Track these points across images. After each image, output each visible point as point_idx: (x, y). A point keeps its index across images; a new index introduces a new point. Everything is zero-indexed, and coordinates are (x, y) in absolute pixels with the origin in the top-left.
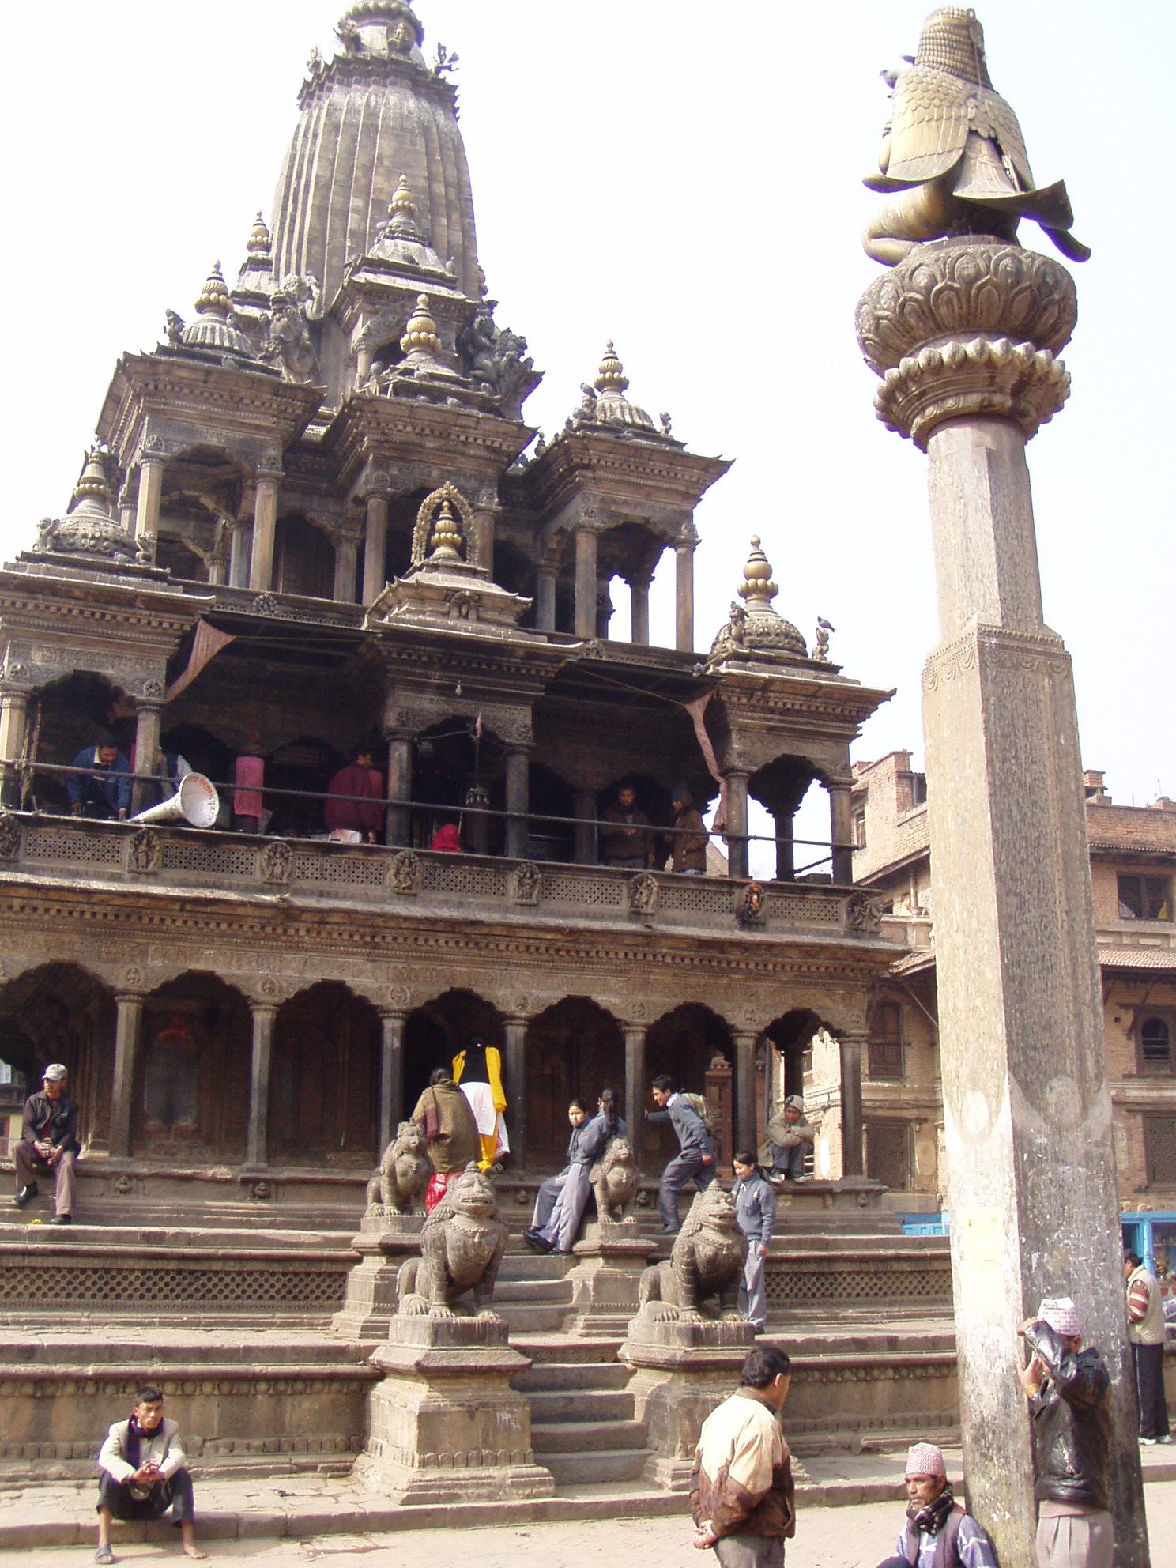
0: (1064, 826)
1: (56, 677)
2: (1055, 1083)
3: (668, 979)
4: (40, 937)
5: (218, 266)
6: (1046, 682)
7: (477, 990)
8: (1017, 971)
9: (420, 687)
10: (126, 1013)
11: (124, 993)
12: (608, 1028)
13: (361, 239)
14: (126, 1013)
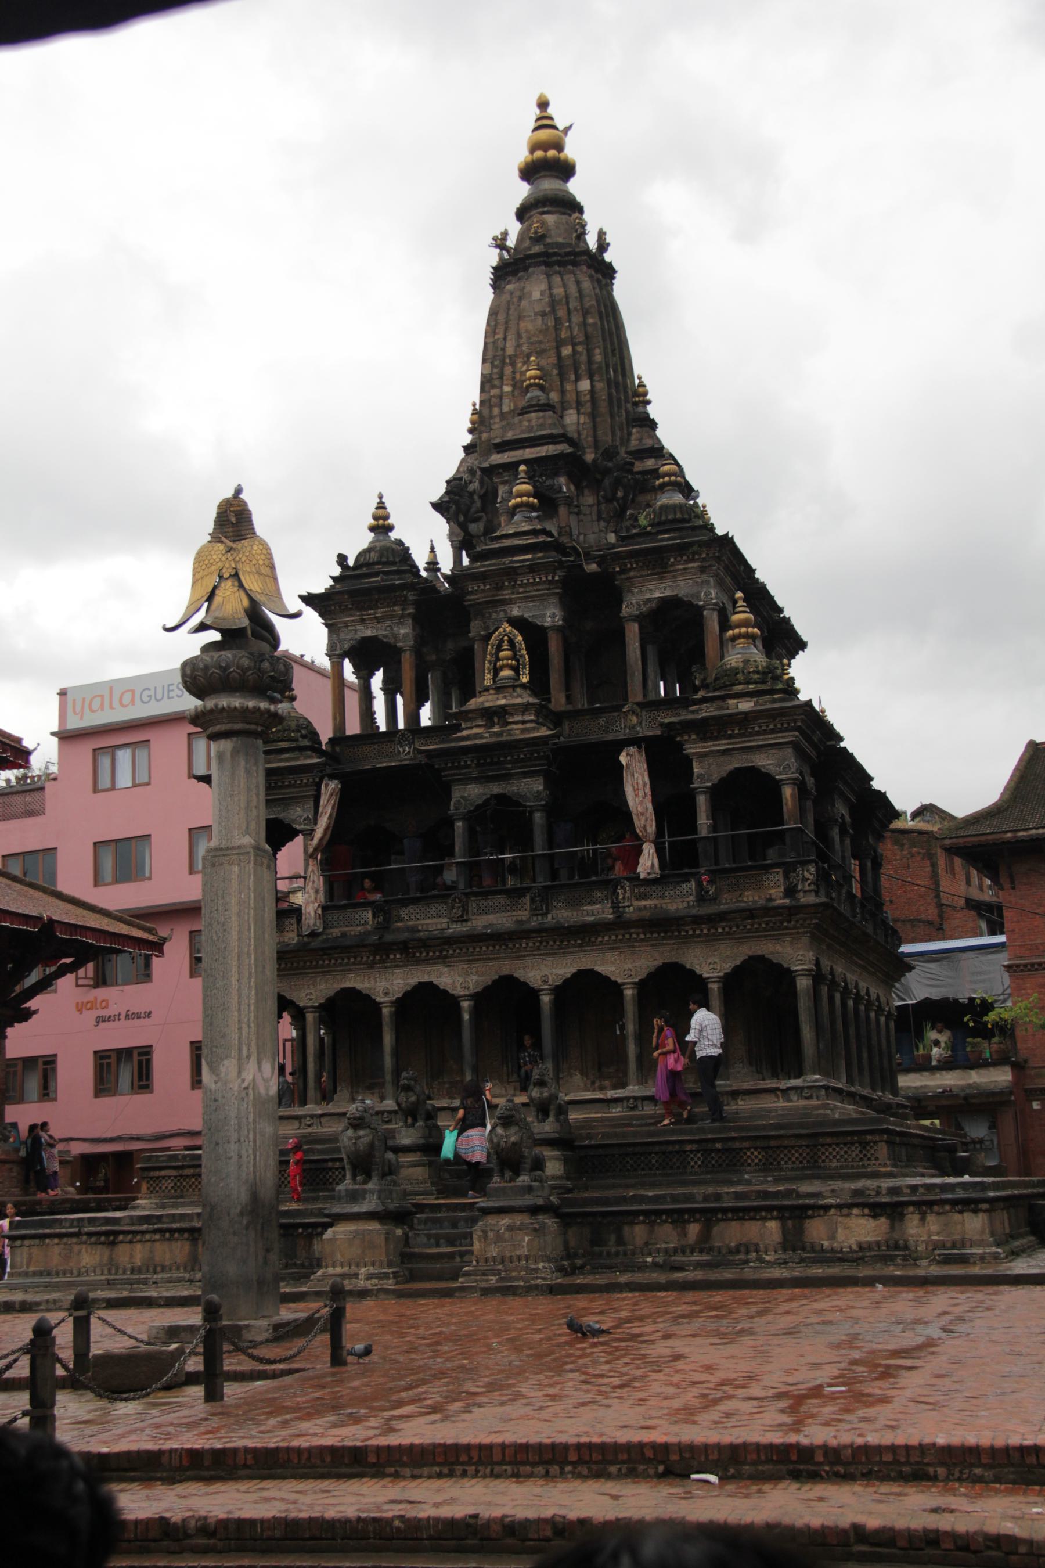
0: (239, 939)
2: (226, 1062)
5: (381, 497)
6: (236, 869)
7: (516, 975)
8: (210, 1012)
9: (466, 780)
11: (308, 1007)
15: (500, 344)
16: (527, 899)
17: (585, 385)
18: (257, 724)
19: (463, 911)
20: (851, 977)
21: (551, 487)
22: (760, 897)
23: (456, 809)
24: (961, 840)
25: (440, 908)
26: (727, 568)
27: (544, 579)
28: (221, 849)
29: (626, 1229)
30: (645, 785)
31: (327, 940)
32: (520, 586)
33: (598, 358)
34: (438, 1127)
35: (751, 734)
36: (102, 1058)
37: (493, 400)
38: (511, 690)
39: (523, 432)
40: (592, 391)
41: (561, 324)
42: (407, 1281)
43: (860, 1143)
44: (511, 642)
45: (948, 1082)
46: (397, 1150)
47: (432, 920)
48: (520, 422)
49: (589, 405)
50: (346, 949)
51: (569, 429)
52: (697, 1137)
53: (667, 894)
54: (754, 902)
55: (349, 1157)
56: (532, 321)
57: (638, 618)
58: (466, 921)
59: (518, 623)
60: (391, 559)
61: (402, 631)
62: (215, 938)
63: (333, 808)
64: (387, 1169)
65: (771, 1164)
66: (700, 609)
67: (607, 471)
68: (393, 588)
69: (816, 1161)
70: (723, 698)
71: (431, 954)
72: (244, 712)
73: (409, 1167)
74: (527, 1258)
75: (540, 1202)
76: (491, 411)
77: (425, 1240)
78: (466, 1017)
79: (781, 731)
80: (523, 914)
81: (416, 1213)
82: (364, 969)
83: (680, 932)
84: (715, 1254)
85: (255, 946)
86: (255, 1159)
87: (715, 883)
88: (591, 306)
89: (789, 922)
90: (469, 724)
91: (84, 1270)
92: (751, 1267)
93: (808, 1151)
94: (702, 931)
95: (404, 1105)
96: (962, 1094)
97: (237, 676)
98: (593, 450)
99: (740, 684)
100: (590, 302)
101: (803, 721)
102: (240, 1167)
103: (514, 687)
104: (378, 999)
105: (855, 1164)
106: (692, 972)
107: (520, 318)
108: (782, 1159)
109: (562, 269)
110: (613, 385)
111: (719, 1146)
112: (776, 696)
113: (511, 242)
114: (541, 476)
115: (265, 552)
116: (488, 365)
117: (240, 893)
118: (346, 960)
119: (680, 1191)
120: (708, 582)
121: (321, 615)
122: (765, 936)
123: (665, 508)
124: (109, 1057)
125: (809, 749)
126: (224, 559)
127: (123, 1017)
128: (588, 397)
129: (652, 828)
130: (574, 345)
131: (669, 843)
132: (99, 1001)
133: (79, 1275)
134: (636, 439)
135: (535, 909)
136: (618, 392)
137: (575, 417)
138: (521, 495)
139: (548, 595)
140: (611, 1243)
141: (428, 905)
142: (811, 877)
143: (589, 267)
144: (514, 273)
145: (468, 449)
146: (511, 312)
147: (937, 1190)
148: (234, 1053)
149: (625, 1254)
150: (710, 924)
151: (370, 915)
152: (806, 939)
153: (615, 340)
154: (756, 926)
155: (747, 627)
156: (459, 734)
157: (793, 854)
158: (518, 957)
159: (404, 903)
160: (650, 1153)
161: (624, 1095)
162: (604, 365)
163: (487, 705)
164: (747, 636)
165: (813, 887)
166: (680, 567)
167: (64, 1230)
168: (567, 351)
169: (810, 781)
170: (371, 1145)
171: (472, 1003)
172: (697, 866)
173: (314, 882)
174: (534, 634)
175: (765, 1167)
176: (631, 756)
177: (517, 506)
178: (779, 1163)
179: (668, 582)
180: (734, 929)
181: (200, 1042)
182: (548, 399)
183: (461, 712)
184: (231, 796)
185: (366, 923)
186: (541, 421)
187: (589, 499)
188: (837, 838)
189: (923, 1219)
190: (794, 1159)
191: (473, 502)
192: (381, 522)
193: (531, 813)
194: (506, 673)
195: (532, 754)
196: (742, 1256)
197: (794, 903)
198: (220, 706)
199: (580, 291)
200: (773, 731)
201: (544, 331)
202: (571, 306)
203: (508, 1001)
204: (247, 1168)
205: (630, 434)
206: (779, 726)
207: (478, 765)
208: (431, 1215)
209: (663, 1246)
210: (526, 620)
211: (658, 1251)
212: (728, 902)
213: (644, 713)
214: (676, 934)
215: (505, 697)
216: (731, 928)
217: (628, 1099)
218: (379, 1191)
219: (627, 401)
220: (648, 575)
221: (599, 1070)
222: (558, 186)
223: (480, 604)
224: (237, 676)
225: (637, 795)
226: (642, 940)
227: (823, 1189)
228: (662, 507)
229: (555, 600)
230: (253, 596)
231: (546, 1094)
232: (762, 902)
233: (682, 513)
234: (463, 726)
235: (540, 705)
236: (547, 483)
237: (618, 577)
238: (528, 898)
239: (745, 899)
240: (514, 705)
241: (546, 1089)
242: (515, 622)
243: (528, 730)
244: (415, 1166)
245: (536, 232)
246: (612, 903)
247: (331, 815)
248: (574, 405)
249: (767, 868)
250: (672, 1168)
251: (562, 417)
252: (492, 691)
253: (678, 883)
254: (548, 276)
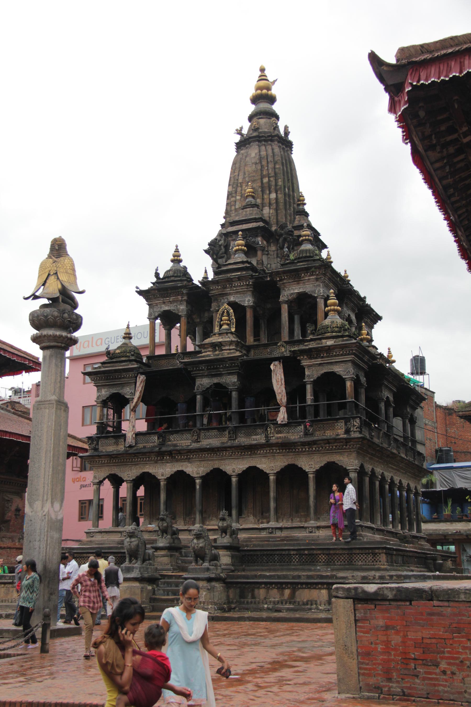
0: (47, 444)
1: (108, 396)
2: (37, 502)
4: (107, 468)
5: (177, 247)
6: (47, 411)
7: (221, 468)
9: (203, 376)
12: (264, 476)
15: (236, 177)
16: (227, 433)
17: (273, 196)
18: (62, 343)
19: (198, 437)
20: (388, 475)
21: (254, 242)
22: (333, 434)
23: (198, 389)
24: (467, 413)
25: (188, 436)
26: (329, 279)
27: (245, 284)
28: (42, 402)
29: (256, 591)
30: (281, 380)
31: (137, 449)
32: (234, 287)
33: (280, 183)
34: (179, 539)
35: (332, 356)
36: (82, 503)
37: (232, 203)
38: (225, 334)
39: (243, 217)
40: (277, 199)
41: (264, 168)
42: (151, 612)
43: (373, 554)
44: (228, 312)
45: (459, 528)
46: (157, 549)
47: (183, 441)
48: (242, 212)
49: (275, 204)
50: (144, 454)
51: (265, 216)
52: (296, 548)
53: (290, 431)
54: (330, 436)
55: (128, 551)
56: (250, 167)
57: (290, 303)
58: (199, 442)
59: (233, 305)
60: (179, 274)
61: (181, 308)
62: (36, 443)
63: (142, 388)
64: (147, 557)
65: (331, 562)
66: (315, 298)
67: (281, 235)
68: (176, 288)
69: (352, 562)
70: (320, 339)
71: (183, 457)
72: (55, 336)
73: (161, 557)
74: (204, 603)
75: (213, 576)
76: (231, 207)
77: (162, 592)
79: (346, 355)
80: (225, 439)
81: (161, 579)
82: (153, 463)
83: (295, 450)
84: (297, 604)
85: (54, 447)
86: (46, 549)
87: (313, 427)
88: (279, 159)
89: (346, 446)
90: (205, 350)
91: (14, 600)
92: (312, 612)
93: (348, 556)
94: (306, 449)
95: (161, 527)
96: (465, 534)
97: (52, 320)
98: (276, 225)
99: (329, 332)
100: (278, 158)
101: (356, 350)
103: (227, 333)
104: (159, 478)
105: (370, 564)
106: (301, 469)
107: (246, 165)
108: (336, 560)
109: (266, 143)
110: (287, 196)
111: (306, 552)
112: (344, 339)
113: (245, 131)
114: (249, 237)
115: (70, 263)
116: (231, 187)
117: (48, 422)
118: (145, 459)
119: (284, 573)
120: (319, 285)
121: (147, 300)
122: (335, 452)
123: (302, 251)
124: (85, 503)
125: (362, 364)
126: (51, 266)
128: (274, 201)
129: (284, 400)
130: (269, 177)
131: (299, 406)
132: (82, 477)
133: (11, 602)
134: (298, 220)
135: (230, 437)
136: (289, 199)
137: (268, 210)
138: (238, 246)
139: (247, 291)
140: (249, 597)
141: (183, 434)
142: (357, 425)
143: (279, 142)
144: (244, 146)
145: (223, 226)
146: (242, 163)
147: (402, 578)
148: (41, 498)
149: (255, 603)
150: (309, 446)
151: (156, 438)
152: (354, 455)
153: (290, 176)
154: (331, 447)
155: (334, 306)
156: (200, 355)
157: (350, 414)
158: (221, 459)
159: (172, 433)
160: (274, 555)
161: (267, 527)
162: (283, 187)
163: (213, 341)
164: (334, 310)
165: (358, 429)
166: (307, 278)
167: (6, 581)
168: (266, 180)
169: (363, 380)
170: (138, 546)
171: (201, 480)
172: (305, 418)
173: (132, 422)
174: (238, 309)
175: (328, 563)
176: (276, 366)
177: (236, 251)
178: (334, 562)
179: (301, 285)
180: (321, 449)
181: (126, 497)
182: (256, 202)
183: (201, 345)
184: (48, 376)
185: (155, 442)
186: (251, 212)
187: (273, 248)
188: (383, 408)
190: (341, 560)
191: (221, 249)
192: (176, 258)
193: (231, 392)
194: (225, 327)
195: (232, 364)
196: (309, 606)
197: (348, 437)
198: (43, 334)
199: (273, 153)
200: (342, 355)
201: (255, 171)
202: (269, 160)
203: (217, 479)
204: (43, 553)
205: (295, 218)
206: (345, 352)
207: (208, 369)
208: (167, 580)
209: (273, 600)
210: (237, 303)
211: (270, 602)
212: (318, 435)
213: (288, 346)
214: (294, 450)
215: (222, 338)
216: (319, 448)
217: (269, 528)
218: (140, 568)
219: (294, 203)
220: (292, 282)
221: (262, 514)
222: (268, 107)
223: (216, 295)
224: (52, 320)
225: (278, 384)
226: (278, 453)
227: (348, 575)
228: (300, 251)
229: (250, 293)
230: (63, 283)
231: (225, 525)
232: (334, 436)
233: (310, 253)
234: (203, 351)
235: (237, 341)
236: (252, 240)
237: (278, 283)
238: (227, 432)
239: (326, 435)
240: (225, 341)
241: (225, 522)
242: (230, 304)
243: (231, 353)
244: (164, 556)
245: (254, 127)
246: (265, 435)
247: (141, 391)
248: (268, 205)
249: (337, 420)
250: (284, 562)
251: (262, 210)
252: (217, 335)
253: (296, 426)
254: (259, 146)
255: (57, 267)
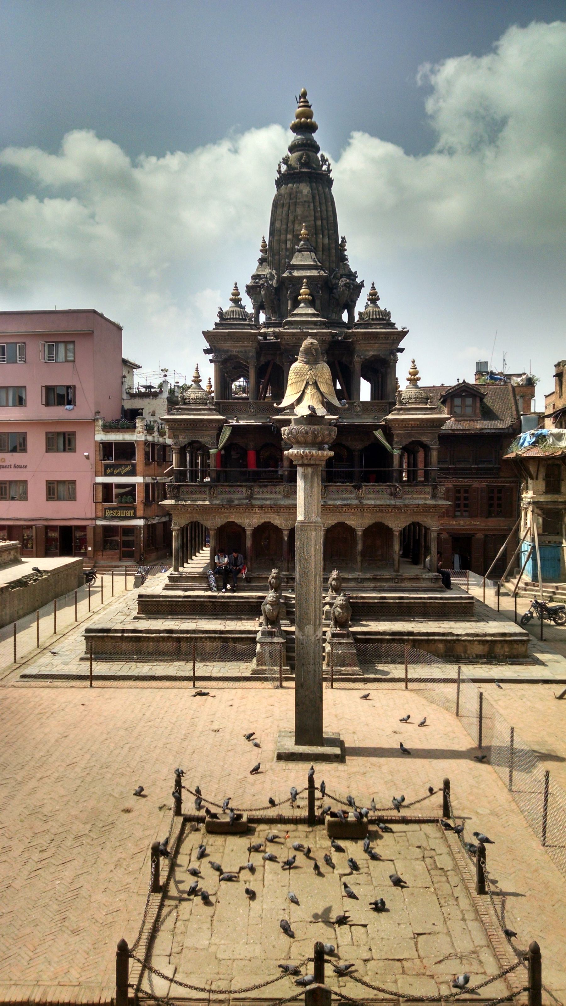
3: (370, 515)
10: (212, 533)
12: (351, 530)
13: (292, 252)
14: (212, 533)
40: (329, 244)
78: (286, 538)
102: (315, 676)
106: (388, 527)
117: (316, 545)
127: (12, 466)
130: (322, 219)
168: (319, 223)
189: (502, 647)
255: (316, 376)
